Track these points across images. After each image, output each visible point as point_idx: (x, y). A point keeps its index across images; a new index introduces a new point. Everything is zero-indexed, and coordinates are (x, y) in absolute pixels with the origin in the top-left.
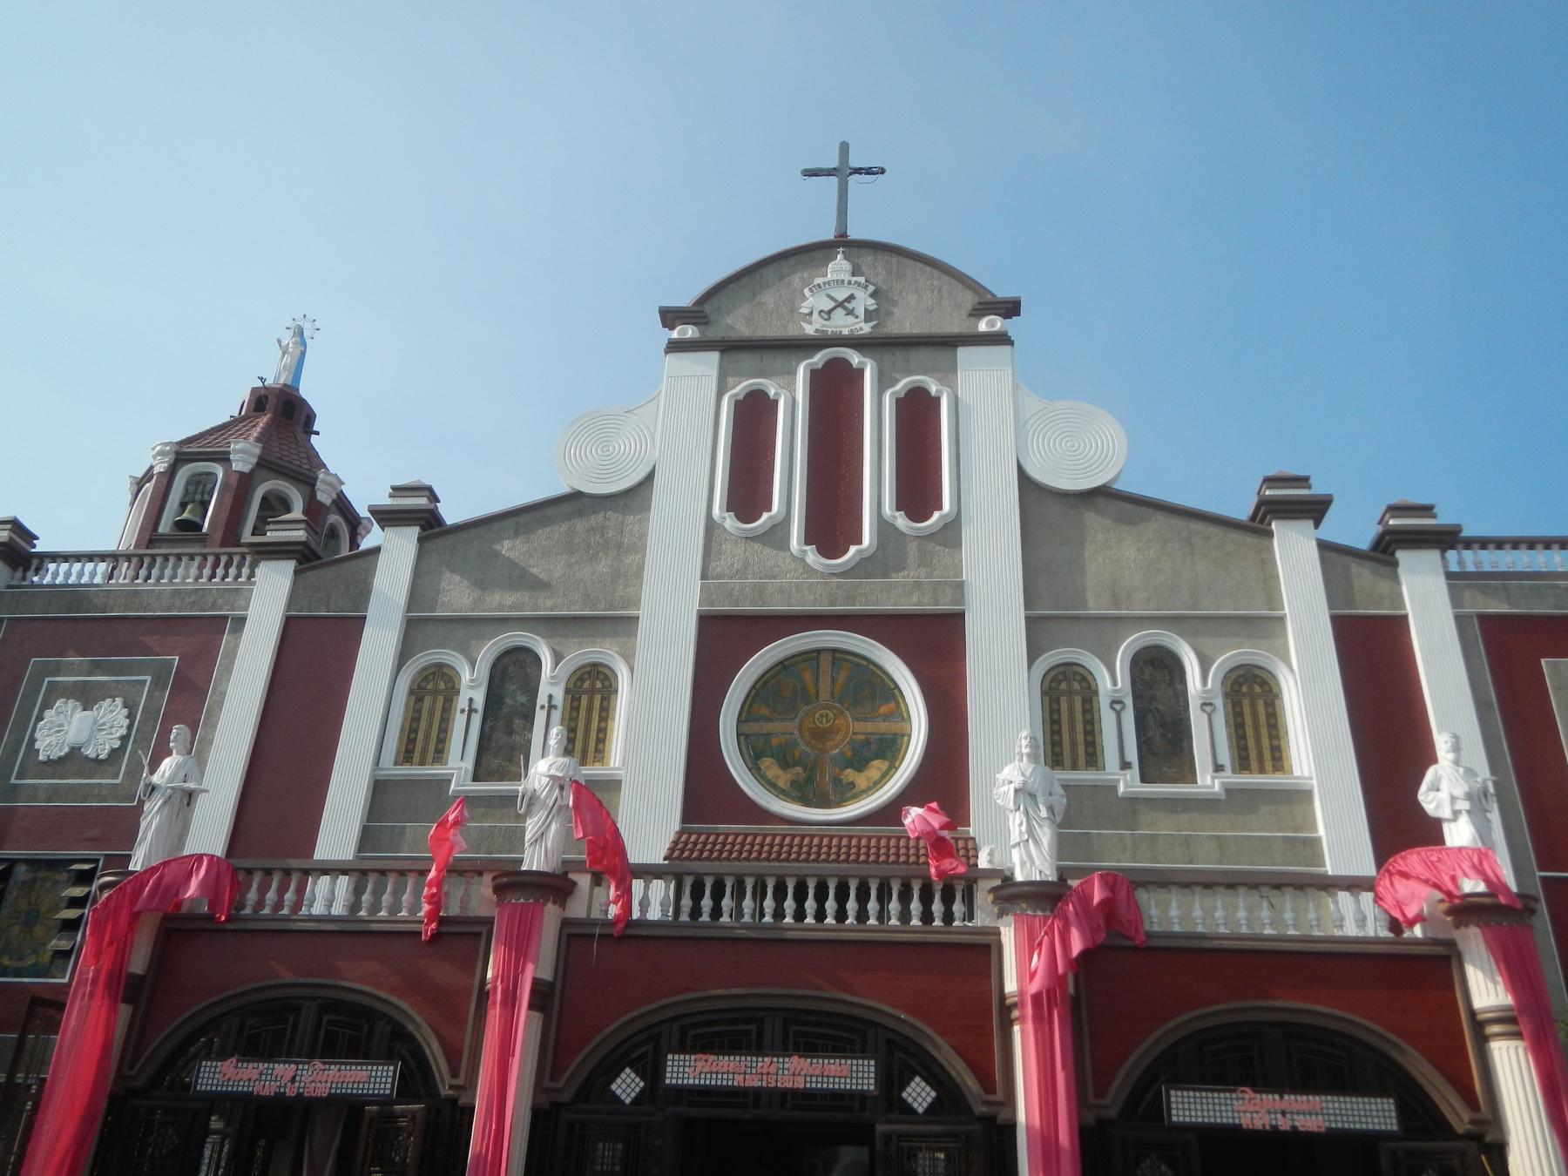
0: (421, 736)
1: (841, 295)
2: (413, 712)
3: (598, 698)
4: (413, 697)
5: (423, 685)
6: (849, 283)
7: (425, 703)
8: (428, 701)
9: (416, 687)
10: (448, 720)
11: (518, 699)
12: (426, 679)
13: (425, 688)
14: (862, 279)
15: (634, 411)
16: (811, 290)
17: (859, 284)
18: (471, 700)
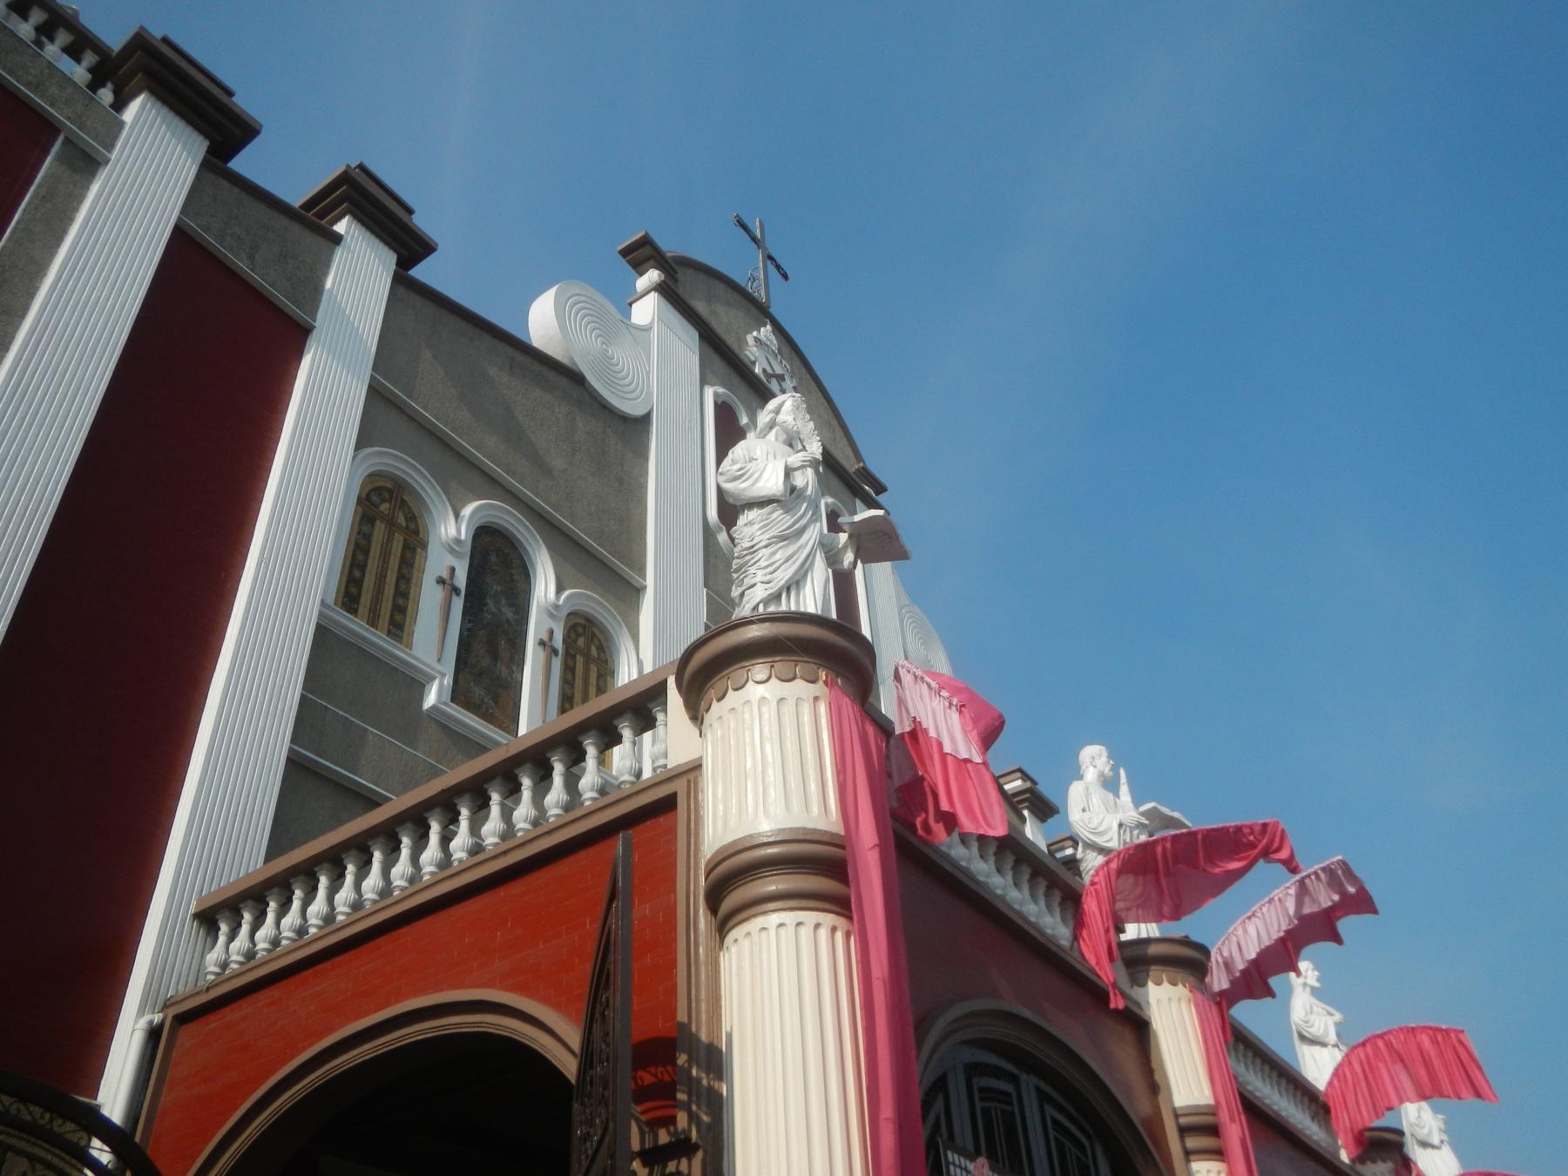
0: (369, 581)
1: (779, 371)
2: (359, 533)
3: (594, 669)
4: (360, 510)
5: (374, 498)
6: (781, 362)
7: (376, 530)
8: (380, 530)
9: (364, 496)
10: (408, 581)
11: (504, 609)
12: (378, 490)
13: (377, 506)
14: (788, 367)
15: (630, 328)
16: (757, 339)
17: (787, 370)
18: (453, 570)
